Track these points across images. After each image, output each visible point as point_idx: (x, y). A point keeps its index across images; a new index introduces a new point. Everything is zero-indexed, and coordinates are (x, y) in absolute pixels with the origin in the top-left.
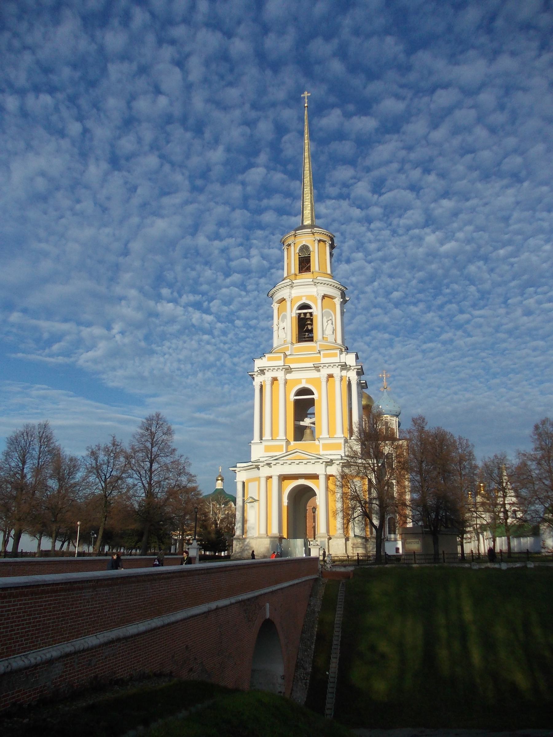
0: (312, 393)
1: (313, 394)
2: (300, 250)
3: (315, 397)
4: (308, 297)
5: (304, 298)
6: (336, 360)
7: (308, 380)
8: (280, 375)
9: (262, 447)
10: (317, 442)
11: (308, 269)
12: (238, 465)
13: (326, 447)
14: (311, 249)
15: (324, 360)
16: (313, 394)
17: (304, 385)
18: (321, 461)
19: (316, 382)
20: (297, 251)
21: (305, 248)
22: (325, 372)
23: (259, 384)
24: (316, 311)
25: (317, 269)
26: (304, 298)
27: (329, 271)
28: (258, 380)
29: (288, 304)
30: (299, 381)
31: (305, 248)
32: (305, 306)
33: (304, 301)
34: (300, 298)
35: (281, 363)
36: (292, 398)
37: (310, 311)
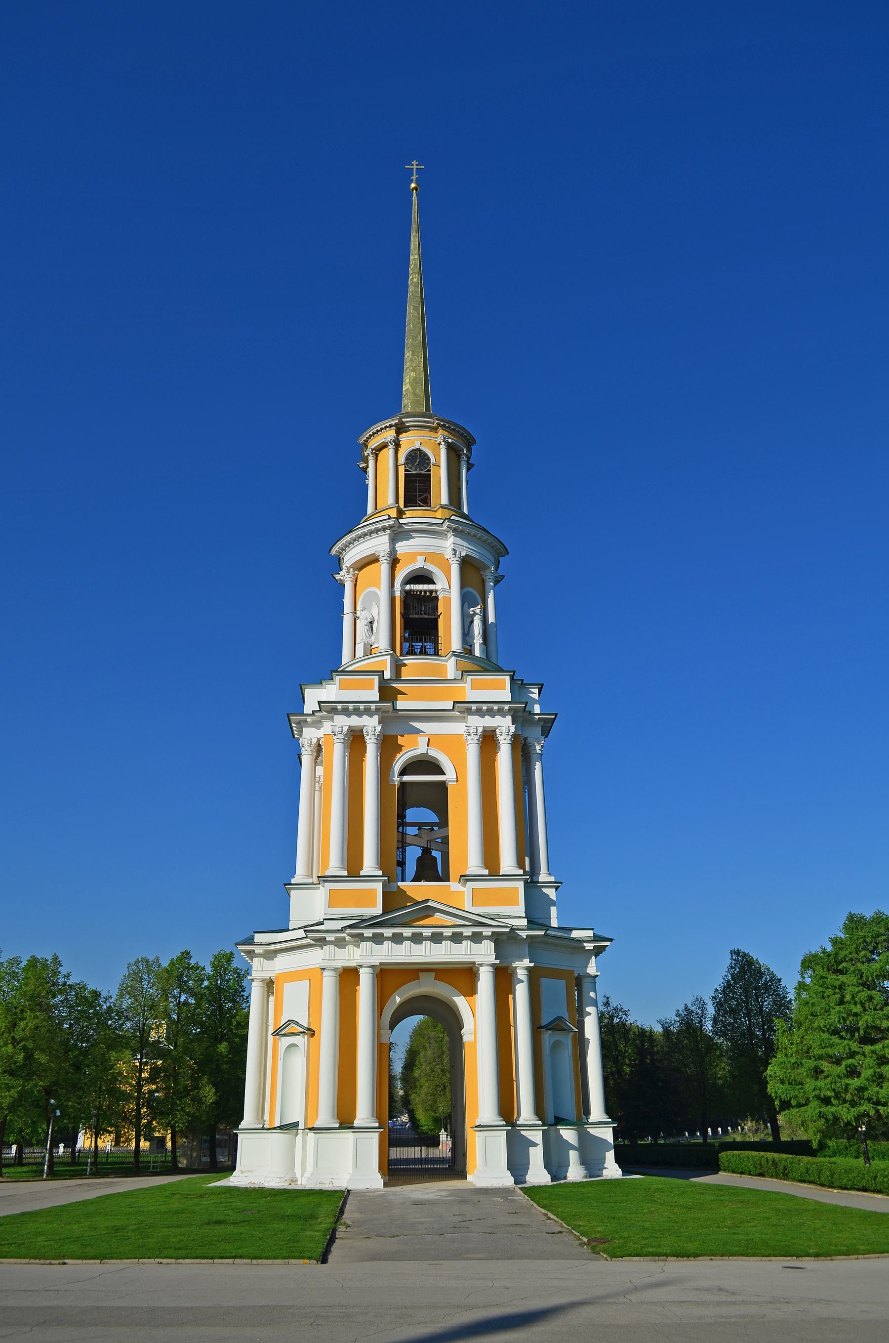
1: (443, 773)
2: (407, 459)
3: (450, 776)
9: (321, 894)
10: (454, 885)
11: (426, 502)
12: (258, 938)
14: (433, 460)
16: (443, 773)
18: (487, 932)
19: (454, 745)
20: (402, 460)
21: (418, 458)
23: (314, 741)
24: (448, 587)
25: (444, 500)
28: (309, 735)
29: (384, 568)
31: (418, 458)
33: (419, 563)
34: (413, 556)
37: (431, 587)
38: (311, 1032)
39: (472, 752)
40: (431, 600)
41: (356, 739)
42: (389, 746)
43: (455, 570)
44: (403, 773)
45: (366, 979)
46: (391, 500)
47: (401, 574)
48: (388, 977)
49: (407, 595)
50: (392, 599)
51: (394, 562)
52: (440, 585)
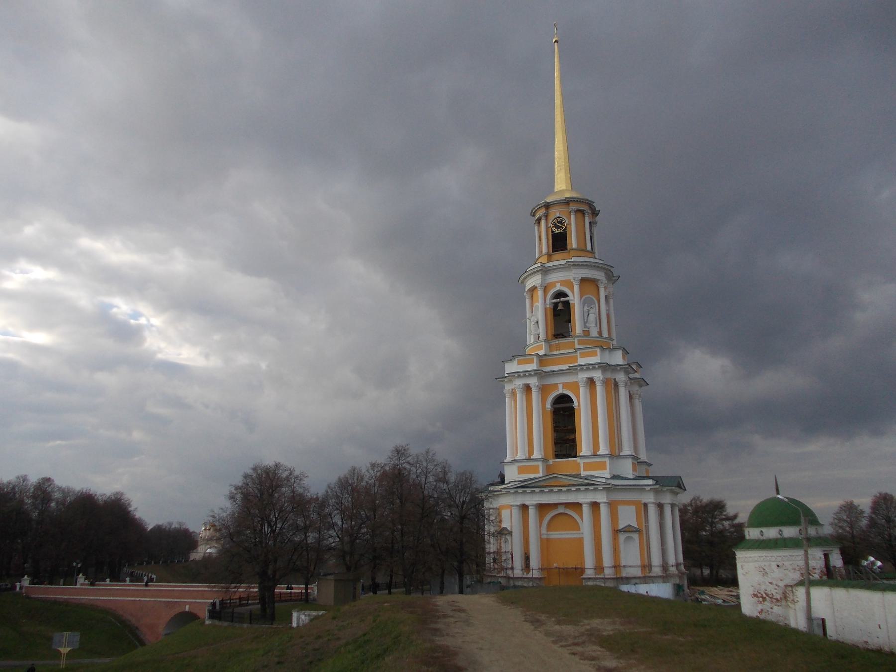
4: (563, 283)
5: (558, 285)
6: (596, 360)
7: (565, 385)
8: (533, 382)
13: (588, 467)
15: (582, 361)
17: (561, 390)
19: (575, 386)
24: (575, 298)
26: (558, 285)
27: (589, 248)
28: (508, 387)
30: (555, 386)
32: (560, 294)
33: (558, 287)
34: (553, 284)
35: (533, 367)
37: (566, 299)
38: (510, 533)
39: (583, 391)
40: (567, 304)
41: (527, 388)
42: (544, 390)
43: (576, 288)
45: (532, 512)
46: (544, 250)
47: (551, 292)
48: (542, 508)
49: (555, 305)
50: (546, 309)
51: (545, 289)
52: (571, 298)
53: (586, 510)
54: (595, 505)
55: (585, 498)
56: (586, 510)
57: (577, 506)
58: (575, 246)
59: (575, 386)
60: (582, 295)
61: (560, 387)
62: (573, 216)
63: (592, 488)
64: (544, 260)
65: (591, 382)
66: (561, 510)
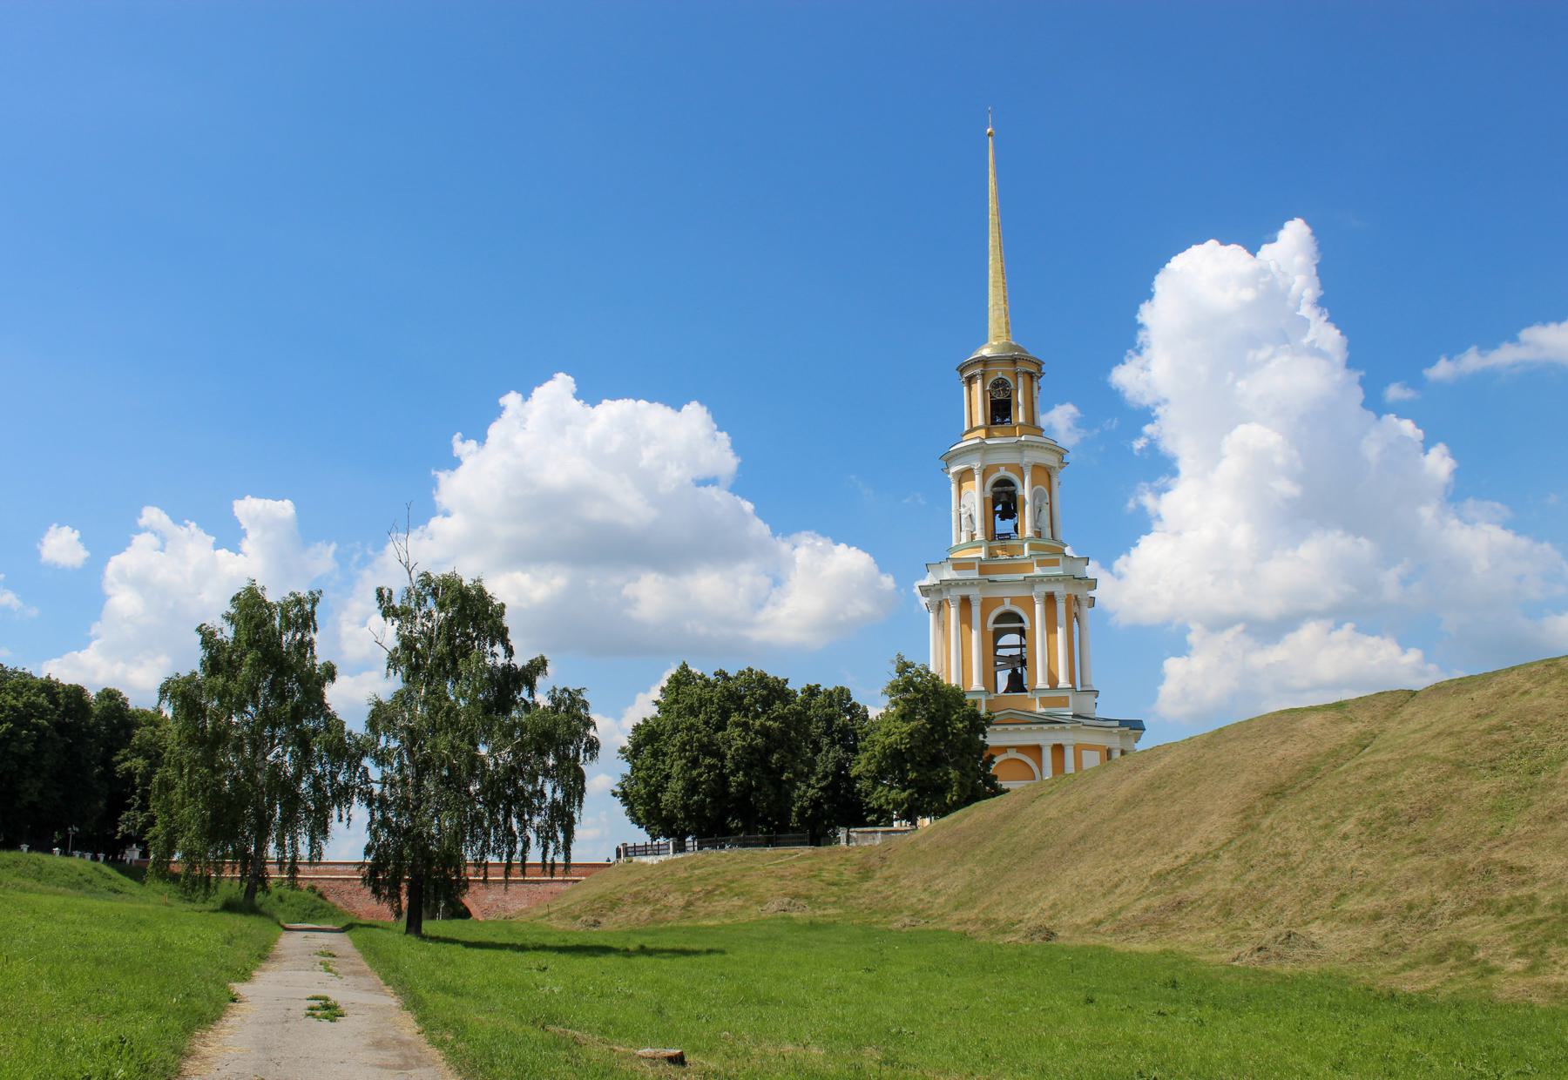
0: (1021, 620)
3: (1027, 626)
4: (1008, 467)
7: (1014, 601)
17: (1008, 606)
22: (1041, 590)
30: (1000, 601)
32: (1004, 483)
36: (991, 626)
39: (1039, 609)
44: (995, 622)
51: (985, 475)
53: (1047, 755)
54: (1058, 749)
55: (1046, 739)
56: (1047, 755)
57: (1036, 750)
58: (1021, 419)
59: (1029, 603)
60: (1033, 485)
61: (1007, 601)
62: (1020, 380)
63: (1057, 726)
64: (982, 433)
65: (1050, 599)
66: (1012, 754)
